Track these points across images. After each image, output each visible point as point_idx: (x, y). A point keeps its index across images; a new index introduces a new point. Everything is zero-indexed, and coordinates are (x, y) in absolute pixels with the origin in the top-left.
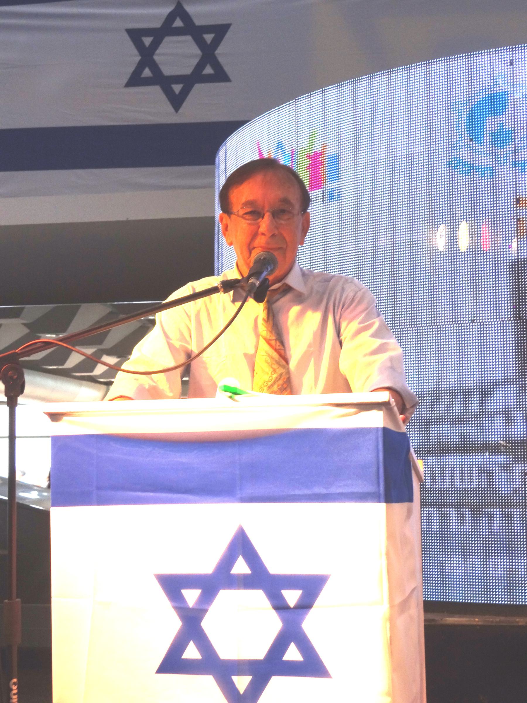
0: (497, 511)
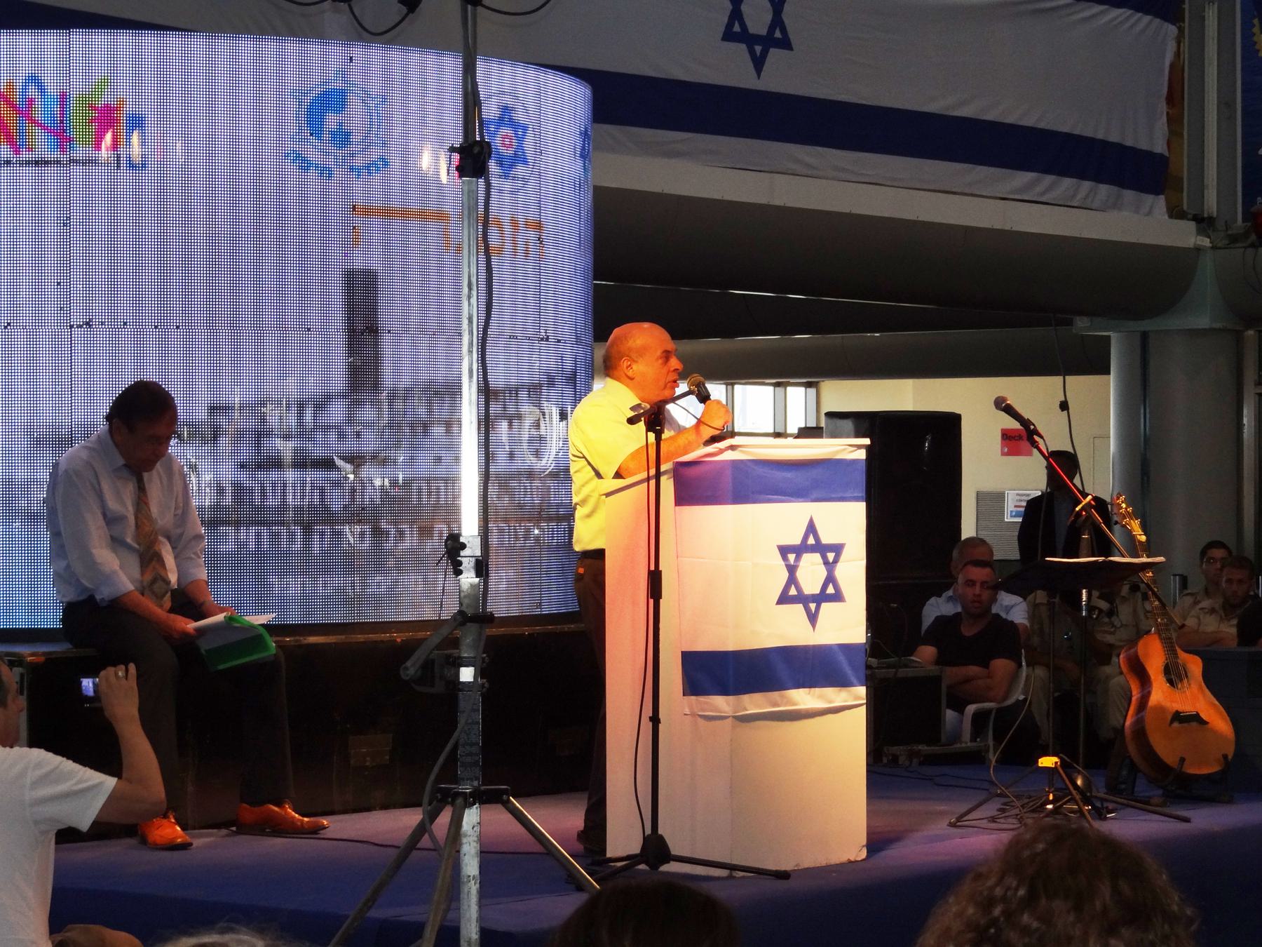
0: (327, 529)
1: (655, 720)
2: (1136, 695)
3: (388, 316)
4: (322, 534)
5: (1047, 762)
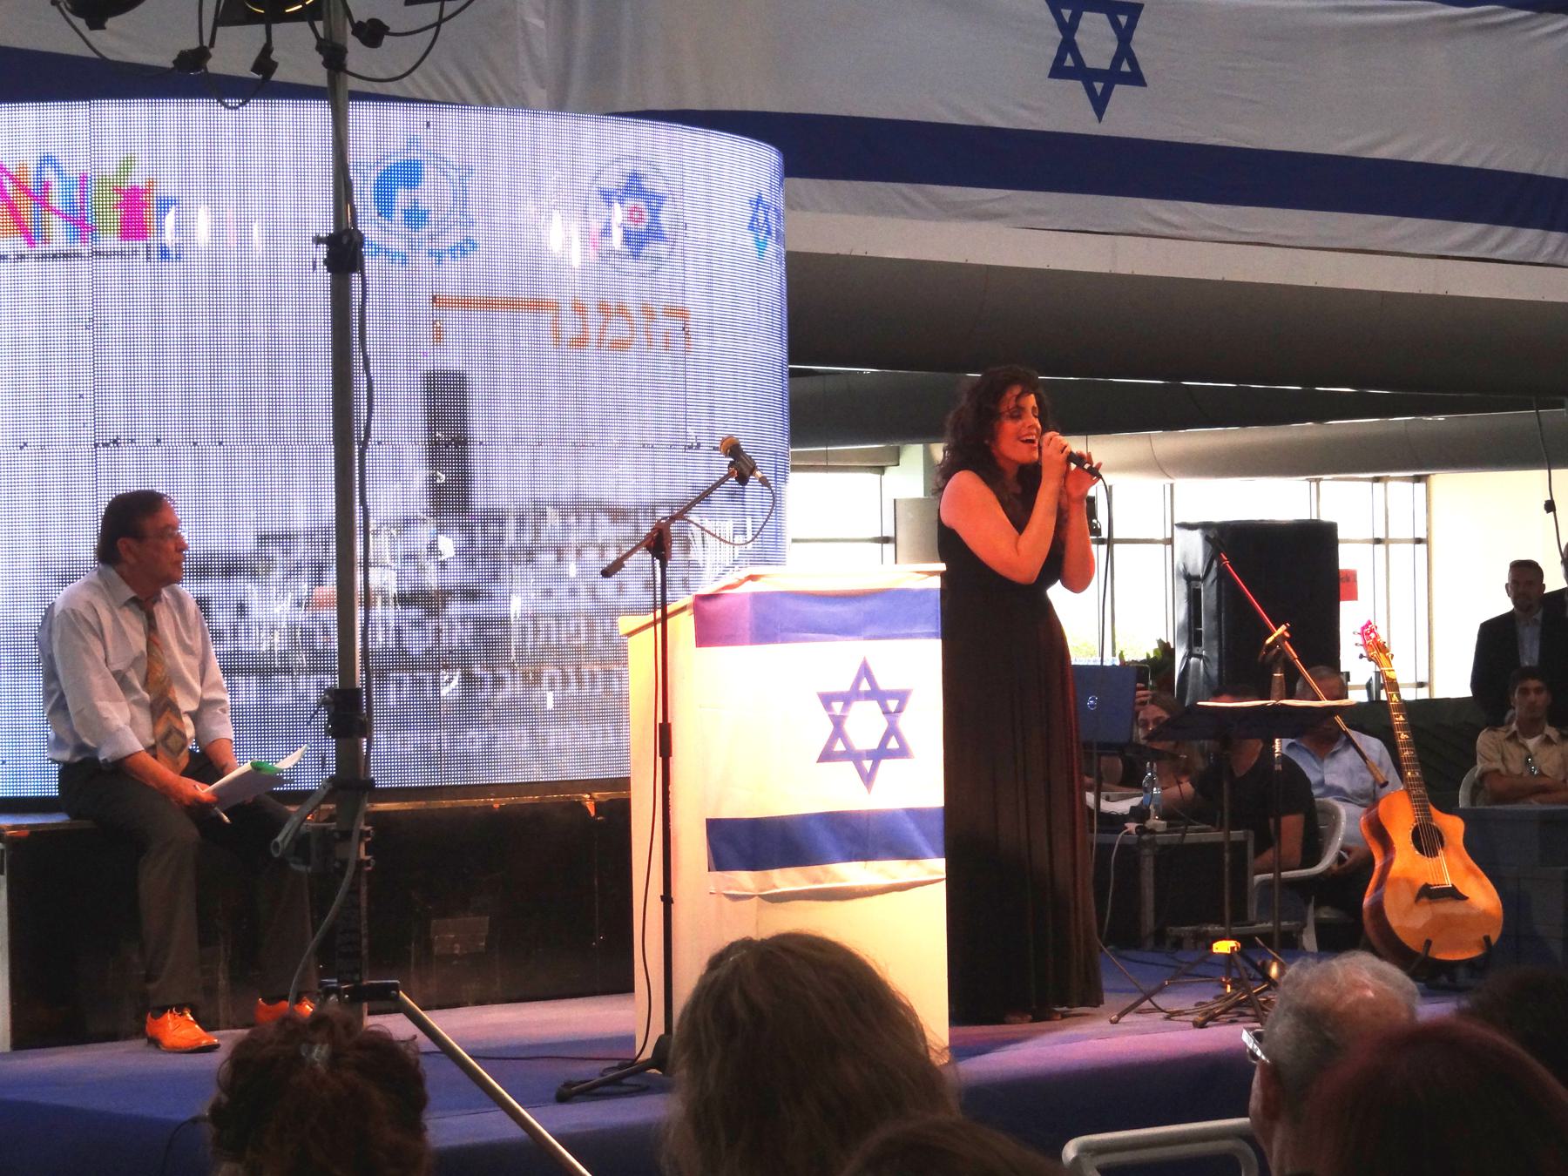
0: (406, 676)
1: (667, 899)
2: (1378, 864)
3: (478, 428)
4: (399, 682)
5: (1223, 947)
